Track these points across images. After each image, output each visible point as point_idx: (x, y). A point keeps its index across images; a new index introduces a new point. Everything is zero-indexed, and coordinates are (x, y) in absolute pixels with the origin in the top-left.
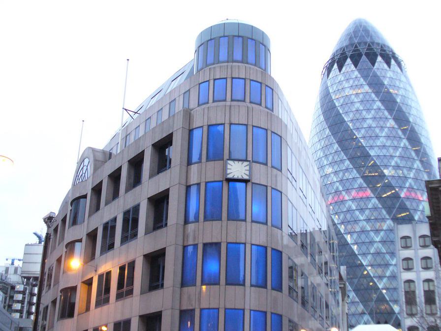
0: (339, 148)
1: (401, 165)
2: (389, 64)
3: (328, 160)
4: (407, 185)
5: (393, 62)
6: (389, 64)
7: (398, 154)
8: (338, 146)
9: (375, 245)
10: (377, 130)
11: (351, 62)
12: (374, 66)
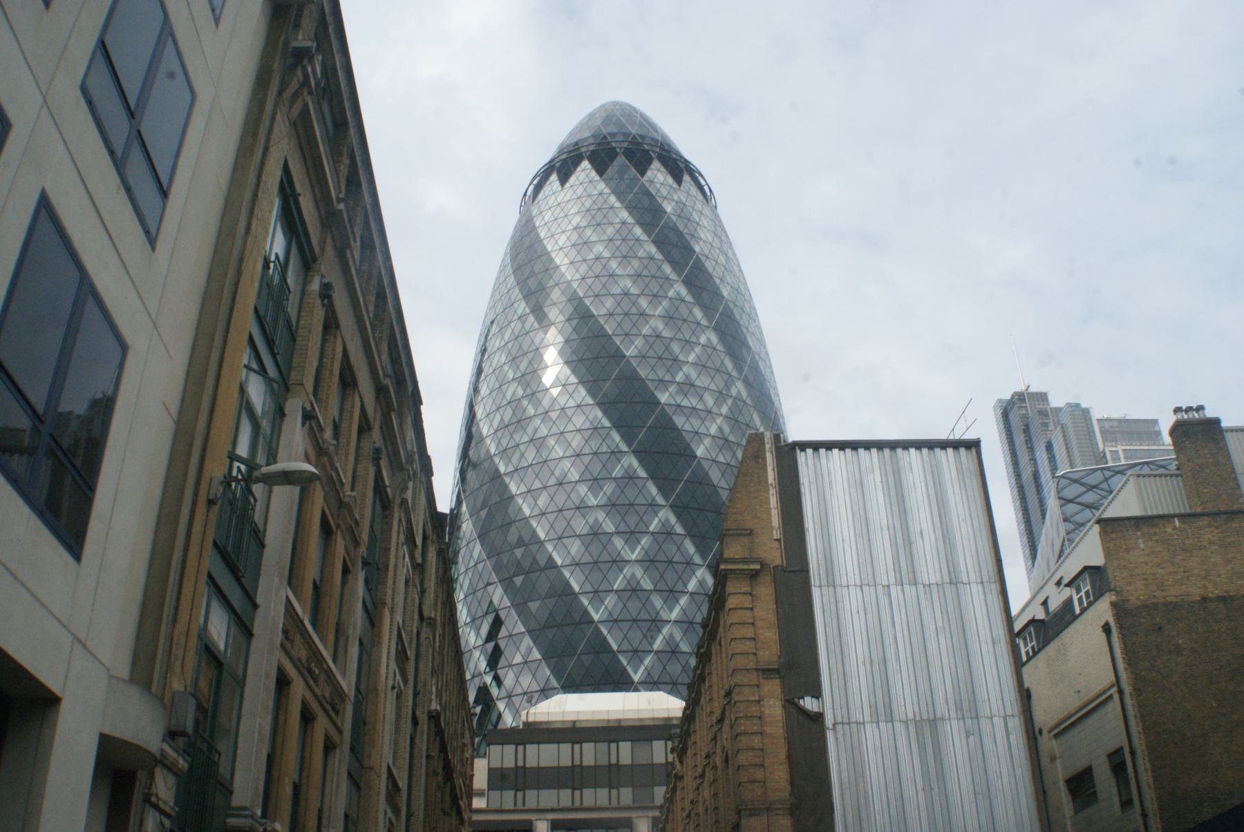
1: (698, 383)
2: (679, 181)
3: (518, 368)
5: (686, 178)
6: (679, 181)
9: (627, 571)
10: (643, 303)
11: (589, 166)
12: (643, 173)
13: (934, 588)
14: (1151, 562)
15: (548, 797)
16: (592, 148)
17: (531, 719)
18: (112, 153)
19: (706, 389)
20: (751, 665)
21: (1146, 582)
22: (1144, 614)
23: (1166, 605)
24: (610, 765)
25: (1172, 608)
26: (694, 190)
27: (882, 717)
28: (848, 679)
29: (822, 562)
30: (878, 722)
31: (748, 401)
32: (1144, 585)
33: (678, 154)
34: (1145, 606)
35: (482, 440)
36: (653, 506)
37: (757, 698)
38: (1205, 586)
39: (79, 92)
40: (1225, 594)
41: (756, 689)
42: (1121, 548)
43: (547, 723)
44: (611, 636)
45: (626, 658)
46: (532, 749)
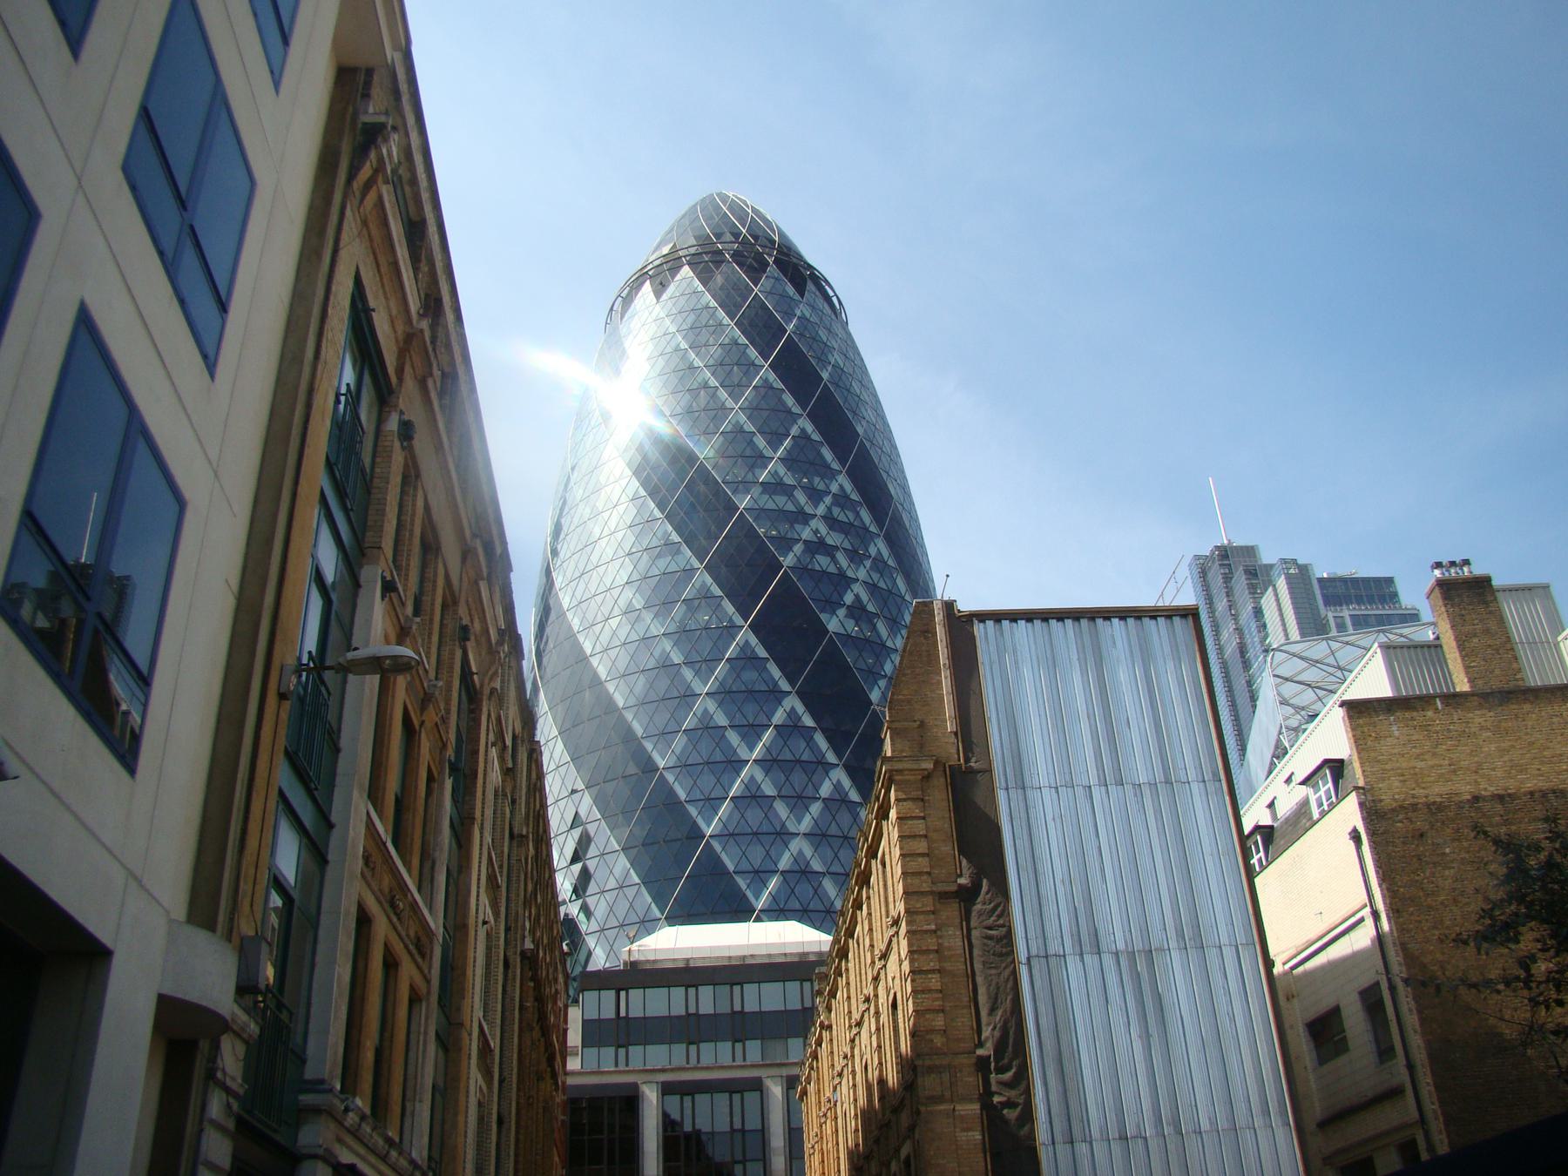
0: (641, 489)
1: (829, 541)
2: (801, 291)
4: (849, 598)
5: (810, 286)
6: (801, 291)
7: (821, 510)
8: (638, 484)
10: (760, 442)
11: (691, 274)
13: (1146, 791)
14: (1408, 753)
15: (656, 1055)
16: (693, 250)
17: (635, 957)
18: (161, 253)
19: (836, 548)
20: (926, 887)
21: (1401, 778)
22: (1401, 817)
23: (1428, 805)
24: (734, 1013)
25: (1435, 808)
26: (821, 303)
27: (1086, 948)
28: (1044, 902)
29: (1008, 759)
30: (1081, 955)
31: (891, 562)
32: (1401, 781)
33: (800, 258)
34: (1401, 807)
35: (562, 615)
36: (777, 695)
37: (933, 927)
38: (1476, 781)
39: (120, 175)
40: (1503, 792)
41: (932, 916)
42: (1370, 736)
43: (655, 961)
44: (726, 853)
45: (744, 879)
46: (636, 994)
